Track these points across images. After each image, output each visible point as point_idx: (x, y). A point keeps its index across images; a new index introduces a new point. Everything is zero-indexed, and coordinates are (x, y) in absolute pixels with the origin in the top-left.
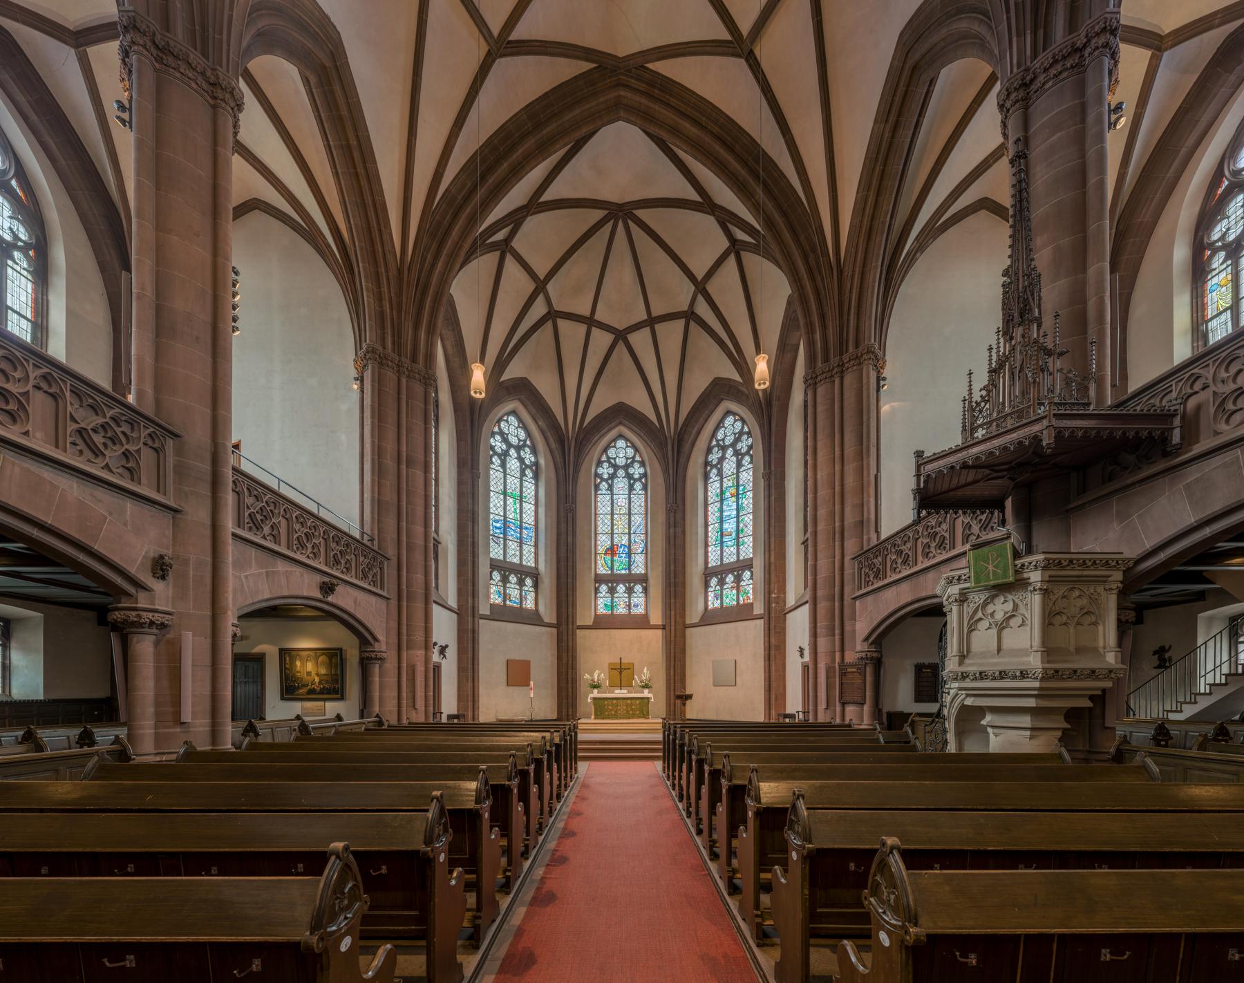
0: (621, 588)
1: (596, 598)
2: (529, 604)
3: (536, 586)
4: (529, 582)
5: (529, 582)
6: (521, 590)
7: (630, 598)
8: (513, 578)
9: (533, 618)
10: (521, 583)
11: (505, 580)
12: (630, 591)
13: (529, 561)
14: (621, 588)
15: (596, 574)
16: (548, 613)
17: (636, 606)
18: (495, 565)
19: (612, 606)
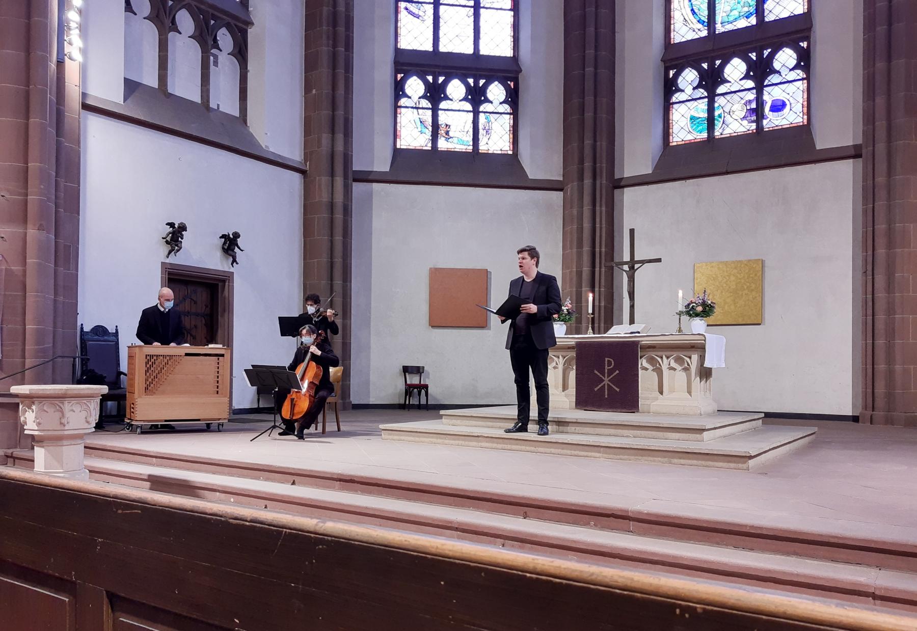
0: (735, 69)
1: (667, 107)
2: (497, 141)
3: (513, 99)
4: (496, 92)
5: (496, 92)
6: (476, 113)
7: (759, 89)
8: (456, 88)
9: (500, 172)
10: (476, 97)
11: (435, 95)
12: (760, 72)
13: (497, 42)
14: (735, 69)
15: (667, 43)
16: (543, 160)
17: (778, 107)
18: (408, 63)
19: (711, 121)
